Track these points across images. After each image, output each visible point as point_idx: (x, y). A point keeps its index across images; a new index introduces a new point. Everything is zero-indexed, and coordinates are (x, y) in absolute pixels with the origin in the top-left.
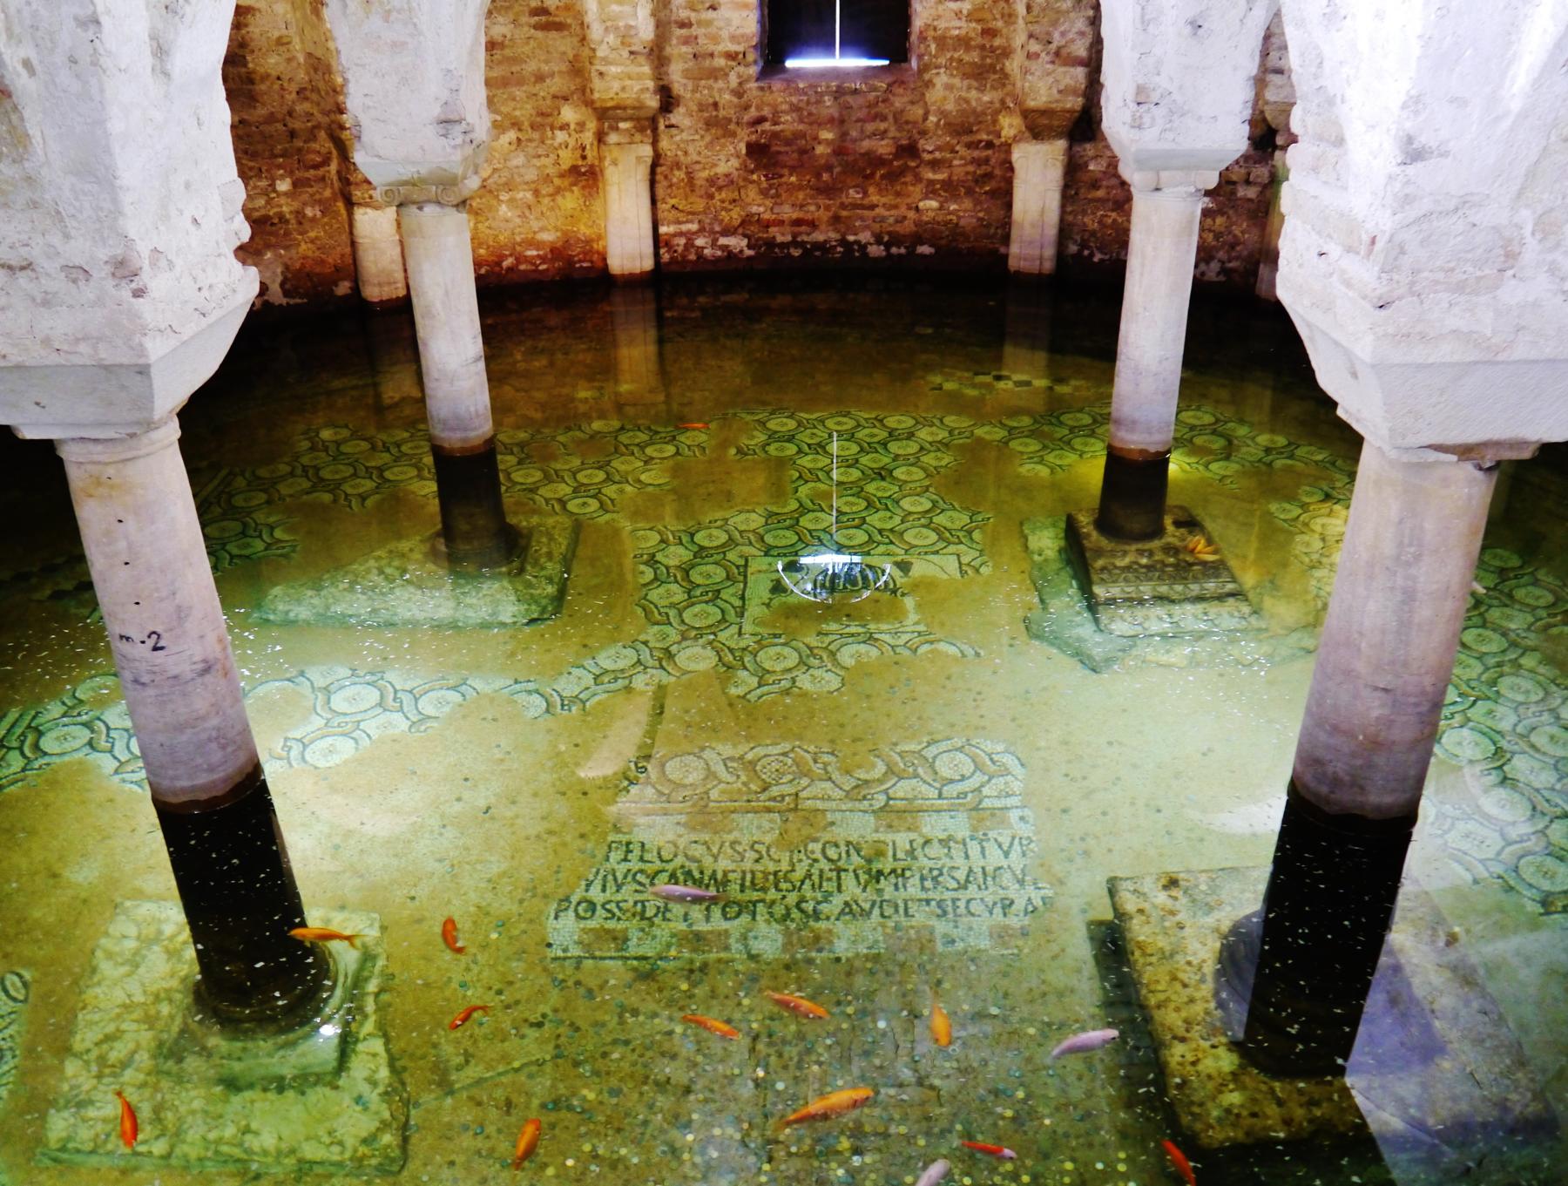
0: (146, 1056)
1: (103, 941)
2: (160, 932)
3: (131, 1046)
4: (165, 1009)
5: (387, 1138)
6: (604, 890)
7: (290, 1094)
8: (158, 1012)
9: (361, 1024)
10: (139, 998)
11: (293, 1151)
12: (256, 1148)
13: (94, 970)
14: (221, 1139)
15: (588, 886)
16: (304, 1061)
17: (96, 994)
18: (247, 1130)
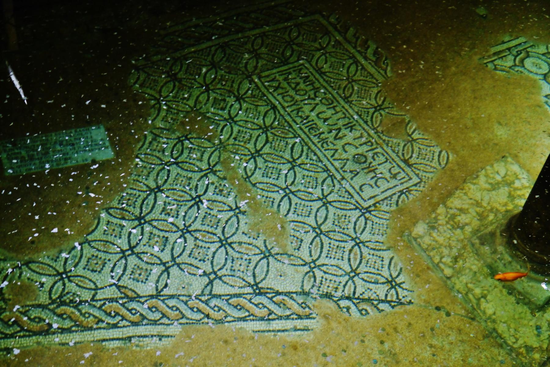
0: (470, 230)
2: (513, 183)
3: (467, 221)
5: (537, 356)
7: (512, 299)
8: (488, 216)
10: (484, 204)
11: (494, 321)
12: (482, 308)
14: (473, 290)
16: (529, 290)
17: (471, 187)
18: (484, 297)
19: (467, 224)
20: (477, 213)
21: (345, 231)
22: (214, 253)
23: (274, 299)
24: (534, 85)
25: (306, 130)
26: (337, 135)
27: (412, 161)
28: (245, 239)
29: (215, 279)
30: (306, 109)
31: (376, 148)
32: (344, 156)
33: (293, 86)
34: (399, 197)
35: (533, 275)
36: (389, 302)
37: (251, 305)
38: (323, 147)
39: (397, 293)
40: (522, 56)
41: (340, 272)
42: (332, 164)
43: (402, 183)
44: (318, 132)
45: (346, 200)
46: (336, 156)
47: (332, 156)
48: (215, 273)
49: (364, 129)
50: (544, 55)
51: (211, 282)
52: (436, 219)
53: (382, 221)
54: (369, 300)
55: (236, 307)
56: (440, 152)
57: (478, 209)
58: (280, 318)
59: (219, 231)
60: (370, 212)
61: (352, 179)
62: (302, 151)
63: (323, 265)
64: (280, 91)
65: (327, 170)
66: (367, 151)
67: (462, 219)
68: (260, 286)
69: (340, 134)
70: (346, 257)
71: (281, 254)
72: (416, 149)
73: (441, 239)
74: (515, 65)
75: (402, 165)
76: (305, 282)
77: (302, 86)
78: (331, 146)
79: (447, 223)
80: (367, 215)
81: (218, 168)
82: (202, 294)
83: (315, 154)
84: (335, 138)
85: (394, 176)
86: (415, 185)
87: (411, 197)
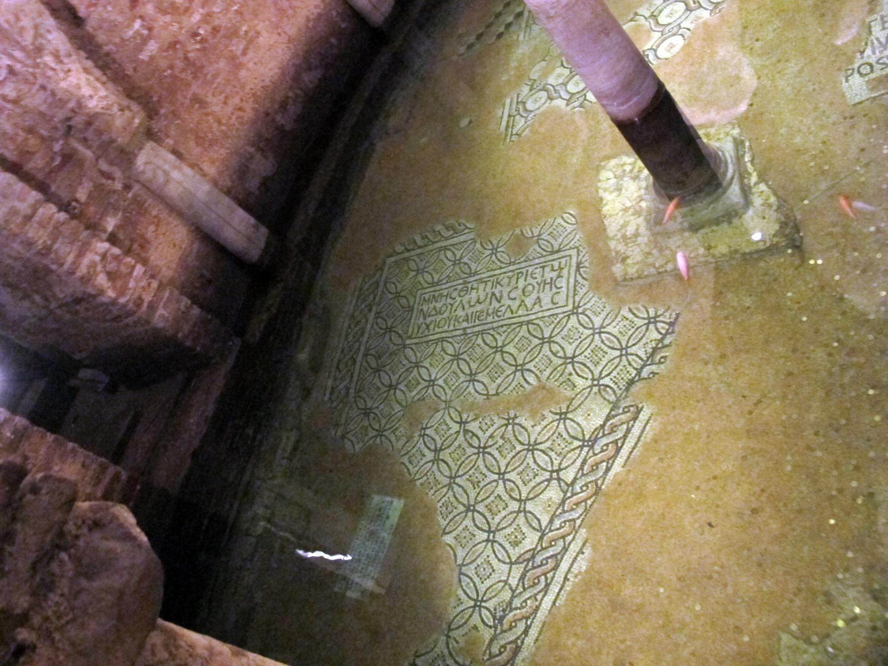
0: (644, 229)
1: (599, 184)
2: (624, 171)
3: (635, 227)
4: (644, 204)
6: (874, 53)
8: (640, 207)
9: (749, 179)
10: (629, 204)
13: (601, 199)
15: (862, 53)
17: (606, 210)
19: (637, 229)
20: (633, 214)
21: (583, 337)
22: (535, 462)
23: (606, 432)
24: (553, 111)
25: (477, 322)
26: (496, 299)
27: (556, 248)
28: (538, 428)
29: (558, 474)
30: (460, 313)
31: (527, 271)
32: (517, 303)
33: (434, 313)
34: (580, 275)
35: (714, 196)
36: (667, 333)
37: (599, 456)
38: (499, 317)
39: (663, 322)
40: (521, 107)
41: (617, 361)
42: (519, 316)
43: (570, 266)
44: (485, 314)
45: (556, 322)
46: (514, 308)
47: (512, 313)
48: (552, 472)
49: (505, 273)
50: (531, 90)
51: (559, 479)
52: (617, 252)
53: (593, 301)
54: (655, 350)
55: (593, 470)
56: (562, 218)
57: (630, 212)
58: (625, 437)
59: (519, 447)
60: (579, 307)
61: (541, 307)
62: (493, 336)
63: (601, 373)
64: (432, 327)
65: (521, 324)
66: (525, 280)
67: (630, 230)
68: (587, 438)
69: (498, 295)
70: (605, 349)
71: (570, 404)
72: (549, 238)
73: (639, 258)
74: (526, 118)
75: (556, 256)
76: (606, 396)
77: (439, 305)
78: (503, 309)
79: (626, 245)
80: (580, 310)
81: (465, 416)
82: (565, 493)
83: (502, 326)
84: (499, 302)
85: (561, 269)
86: (578, 255)
87: (587, 264)
